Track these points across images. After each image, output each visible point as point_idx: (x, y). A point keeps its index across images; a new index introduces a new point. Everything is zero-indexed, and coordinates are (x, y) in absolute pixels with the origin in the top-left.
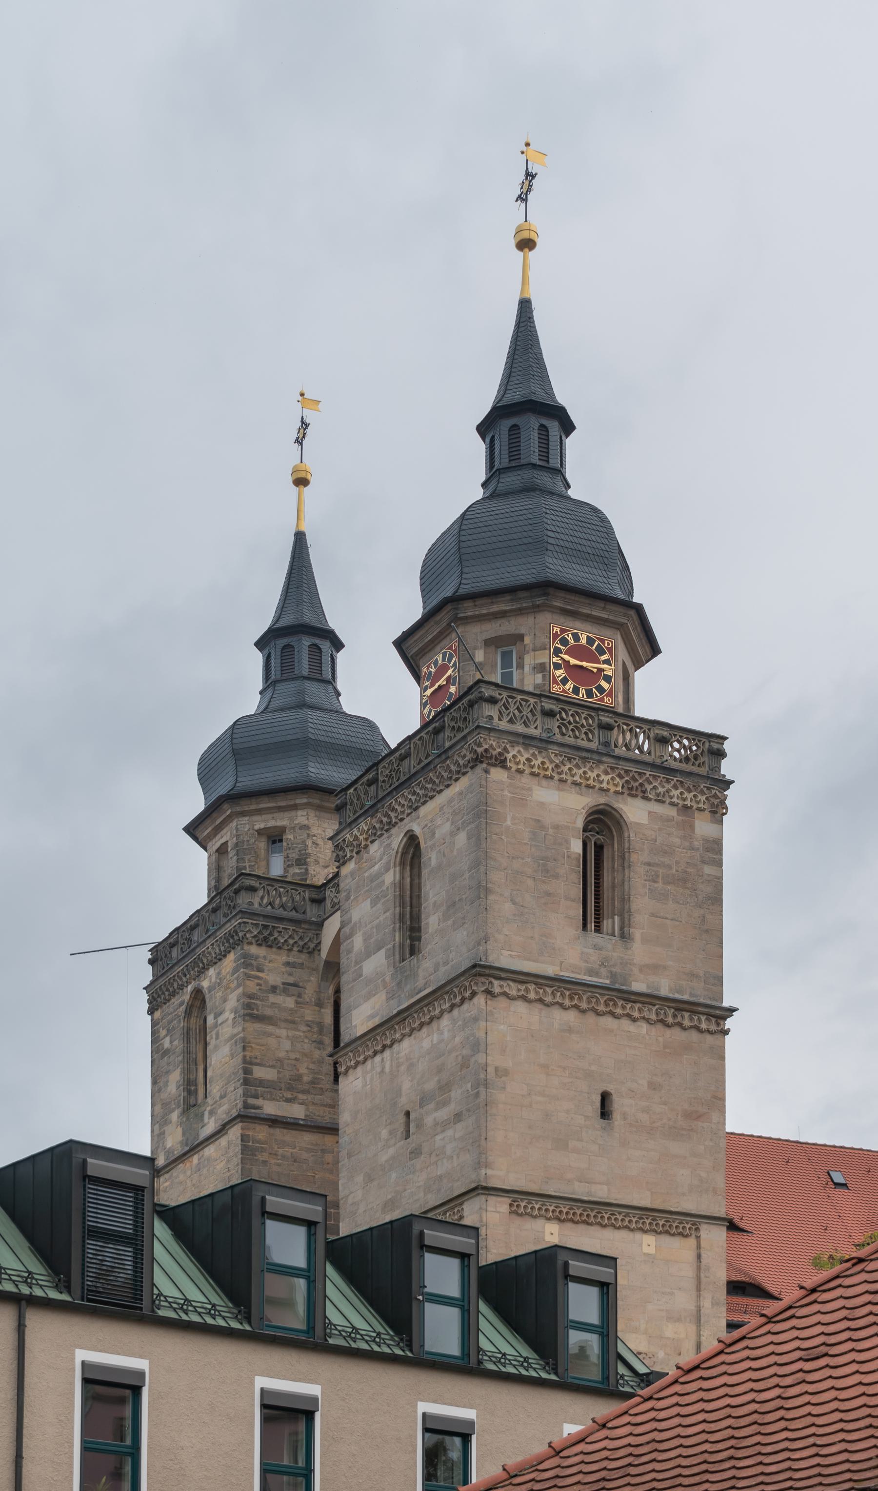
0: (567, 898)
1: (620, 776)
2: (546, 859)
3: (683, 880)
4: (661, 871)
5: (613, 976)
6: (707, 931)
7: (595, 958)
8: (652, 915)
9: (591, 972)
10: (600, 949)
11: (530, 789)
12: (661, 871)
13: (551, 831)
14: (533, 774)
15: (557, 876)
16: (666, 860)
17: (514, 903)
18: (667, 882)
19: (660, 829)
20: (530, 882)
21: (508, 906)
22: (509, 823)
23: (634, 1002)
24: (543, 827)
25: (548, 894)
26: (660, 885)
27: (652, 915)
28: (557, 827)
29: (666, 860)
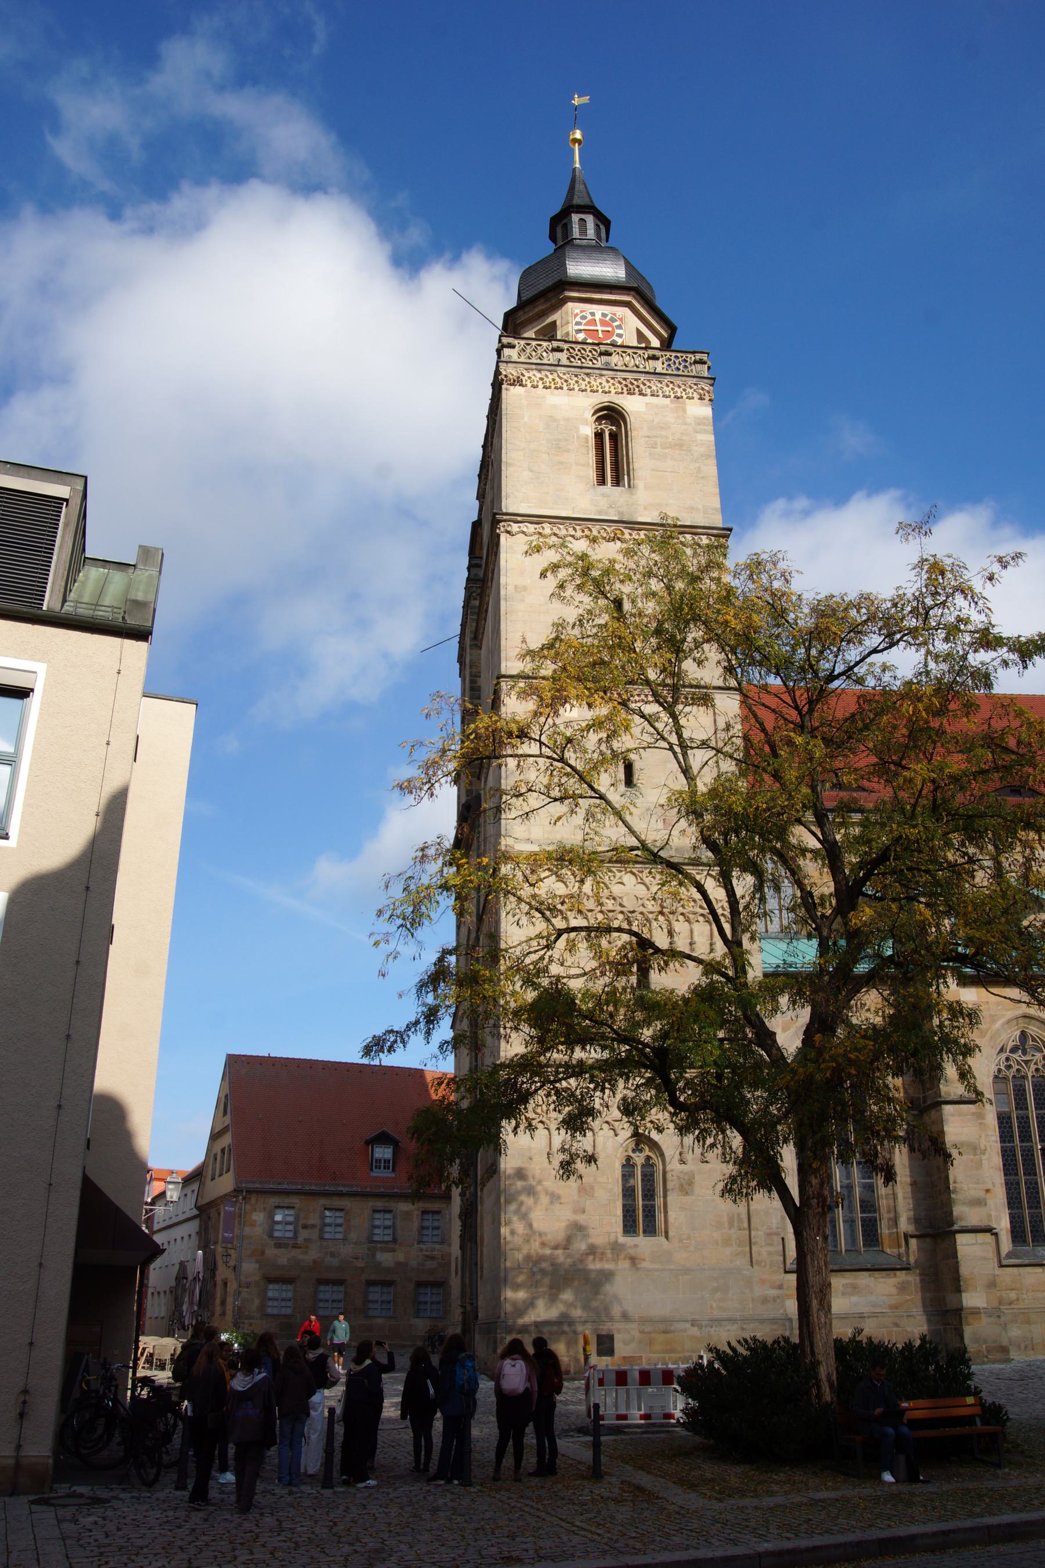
0: (577, 464)
1: (620, 383)
2: (559, 440)
3: (680, 445)
4: (659, 440)
5: (619, 513)
6: (703, 478)
7: (603, 503)
8: (654, 470)
9: (600, 512)
10: (608, 496)
11: (544, 397)
12: (659, 440)
13: (562, 422)
14: (545, 387)
15: (568, 451)
16: (663, 433)
17: (531, 471)
18: (664, 446)
19: (656, 414)
20: (545, 457)
21: (526, 475)
22: (526, 419)
23: (640, 530)
24: (555, 420)
25: (562, 463)
26: (659, 449)
27: (654, 470)
28: (567, 419)
29: (663, 433)
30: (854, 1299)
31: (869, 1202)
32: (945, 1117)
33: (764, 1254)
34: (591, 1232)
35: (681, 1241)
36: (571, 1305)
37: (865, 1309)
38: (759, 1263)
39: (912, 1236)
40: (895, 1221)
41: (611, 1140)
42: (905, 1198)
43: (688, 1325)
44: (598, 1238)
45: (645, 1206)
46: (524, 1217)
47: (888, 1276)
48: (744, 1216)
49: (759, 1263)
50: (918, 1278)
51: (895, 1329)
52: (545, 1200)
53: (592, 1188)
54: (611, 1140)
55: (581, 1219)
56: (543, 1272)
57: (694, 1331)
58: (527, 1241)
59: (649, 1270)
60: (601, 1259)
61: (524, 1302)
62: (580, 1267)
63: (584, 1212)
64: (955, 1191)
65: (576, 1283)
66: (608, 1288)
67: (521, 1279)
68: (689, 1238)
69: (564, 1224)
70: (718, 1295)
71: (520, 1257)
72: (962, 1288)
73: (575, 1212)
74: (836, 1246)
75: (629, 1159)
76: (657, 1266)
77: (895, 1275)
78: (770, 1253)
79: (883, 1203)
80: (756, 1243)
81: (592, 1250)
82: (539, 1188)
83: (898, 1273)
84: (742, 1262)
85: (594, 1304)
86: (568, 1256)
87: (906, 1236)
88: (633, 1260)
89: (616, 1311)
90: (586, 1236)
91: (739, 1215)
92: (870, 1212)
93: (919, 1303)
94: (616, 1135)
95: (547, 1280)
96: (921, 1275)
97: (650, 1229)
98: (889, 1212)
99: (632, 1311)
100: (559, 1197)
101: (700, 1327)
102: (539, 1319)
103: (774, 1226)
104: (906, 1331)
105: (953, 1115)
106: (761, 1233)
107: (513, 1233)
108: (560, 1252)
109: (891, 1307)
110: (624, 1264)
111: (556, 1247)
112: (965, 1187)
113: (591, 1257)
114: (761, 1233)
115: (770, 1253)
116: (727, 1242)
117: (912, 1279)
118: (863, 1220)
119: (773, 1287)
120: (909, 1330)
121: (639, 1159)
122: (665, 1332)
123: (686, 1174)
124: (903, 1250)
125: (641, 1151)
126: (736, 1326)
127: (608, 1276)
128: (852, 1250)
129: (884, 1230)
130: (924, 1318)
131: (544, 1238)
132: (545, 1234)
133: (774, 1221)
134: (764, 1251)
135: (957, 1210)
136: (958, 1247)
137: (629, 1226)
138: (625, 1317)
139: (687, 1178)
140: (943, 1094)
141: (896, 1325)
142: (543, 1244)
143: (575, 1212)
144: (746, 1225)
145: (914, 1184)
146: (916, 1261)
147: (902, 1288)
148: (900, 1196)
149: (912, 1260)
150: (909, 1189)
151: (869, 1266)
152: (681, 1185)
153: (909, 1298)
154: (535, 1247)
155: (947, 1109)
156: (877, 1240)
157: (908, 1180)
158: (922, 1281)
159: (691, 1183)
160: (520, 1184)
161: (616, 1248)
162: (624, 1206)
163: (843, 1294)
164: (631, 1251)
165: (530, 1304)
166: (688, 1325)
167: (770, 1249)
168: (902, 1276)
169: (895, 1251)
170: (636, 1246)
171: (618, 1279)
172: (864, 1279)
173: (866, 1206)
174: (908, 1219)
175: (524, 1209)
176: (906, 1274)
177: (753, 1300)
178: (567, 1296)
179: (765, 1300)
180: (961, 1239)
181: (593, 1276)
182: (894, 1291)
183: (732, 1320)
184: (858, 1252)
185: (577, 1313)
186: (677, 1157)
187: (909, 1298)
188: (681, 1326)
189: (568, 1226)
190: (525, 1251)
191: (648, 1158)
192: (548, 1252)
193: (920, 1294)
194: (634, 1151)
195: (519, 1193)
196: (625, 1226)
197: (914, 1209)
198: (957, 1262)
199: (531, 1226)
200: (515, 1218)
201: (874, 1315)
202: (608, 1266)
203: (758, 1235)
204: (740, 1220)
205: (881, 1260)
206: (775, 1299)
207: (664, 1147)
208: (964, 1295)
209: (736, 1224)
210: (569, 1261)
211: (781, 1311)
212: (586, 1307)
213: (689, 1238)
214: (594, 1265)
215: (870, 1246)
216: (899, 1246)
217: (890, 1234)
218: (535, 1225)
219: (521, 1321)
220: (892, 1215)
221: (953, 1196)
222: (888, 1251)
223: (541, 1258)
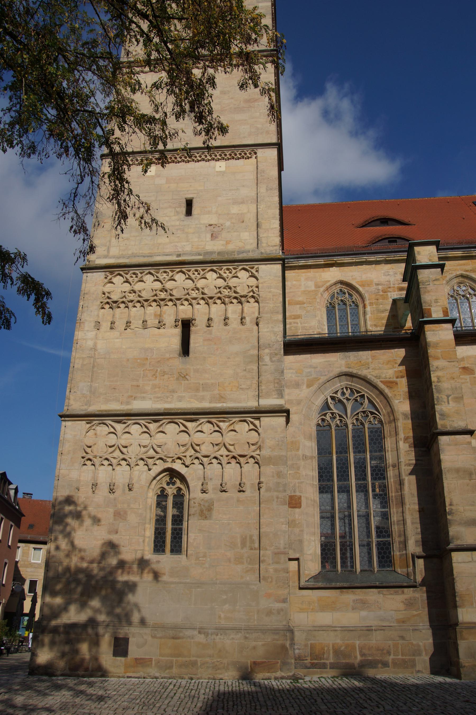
30: (364, 613)
31: (384, 528)
32: (441, 447)
33: (271, 570)
34: (122, 549)
35: (197, 558)
36: (97, 611)
37: (374, 623)
38: (265, 579)
39: (419, 557)
40: (404, 544)
41: (145, 473)
42: (413, 523)
43: (196, 632)
44: (128, 555)
45: (173, 530)
46: (68, 535)
47: (396, 593)
48: (256, 538)
49: (265, 579)
50: (425, 595)
51: (401, 642)
52: (88, 522)
53: (126, 513)
54: (145, 473)
55: (115, 538)
56: (78, 582)
57: (201, 638)
58: (68, 556)
59: (166, 583)
60: (129, 573)
61: (59, 606)
62: (111, 578)
63: (117, 532)
64: (451, 513)
65: (103, 592)
66: (131, 598)
67: (59, 587)
68: (205, 556)
69: (100, 543)
70: (227, 607)
71: (60, 569)
72: (458, 604)
73: (110, 532)
74: (352, 567)
75: (163, 490)
76: (176, 580)
77: (403, 592)
78: (276, 570)
79: (395, 529)
80: (264, 561)
81: (122, 564)
82: (84, 513)
83: (406, 590)
84: (251, 578)
85: (118, 610)
86: (102, 569)
87: (414, 557)
88: (156, 576)
89: (136, 617)
90: (117, 553)
91: (251, 537)
92: (384, 537)
93: (426, 618)
94: (150, 470)
95: (79, 589)
96: (427, 592)
97: (177, 548)
98: (400, 536)
99: (150, 620)
100: (99, 520)
101: (207, 634)
102: (69, 622)
103: (282, 546)
104: (412, 644)
105: (449, 445)
106: (269, 552)
107: (57, 548)
108: (95, 565)
109: (398, 621)
110: (148, 577)
111: (92, 562)
112: (461, 509)
113: (120, 571)
114: (269, 552)
115: (276, 570)
116: (239, 560)
117: (420, 595)
118: (378, 544)
119: (280, 602)
120: (414, 643)
121: (171, 491)
122: (173, 638)
123: (207, 501)
124: (411, 569)
125: (174, 484)
126: (239, 635)
127: (132, 587)
128: (368, 570)
129: (396, 553)
130: (430, 632)
131: (83, 554)
132: (85, 550)
133: (282, 542)
134: (271, 569)
135: (453, 530)
136: (454, 565)
137: (159, 546)
138: (143, 622)
139: (207, 504)
140: (439, 427)
141: (402, 638)
142: (82, 559)
143: (110, 532)
144: (257, 545)
145: (421, 511)
146: (423, 580)
147: (409, 604)
148: (409, 521)
149: (419, 578)
150: (417, 515)
151: (377, 584)
152: (202, 511)
153: (415, 613)
154: (74, 561)
155: (443, 440)
156: (390, 561)
157: (417, 507)
158: (428, 597)
159: (210, 509)
160: (68, 508)
161: (143, 563)
162: (156, 529)
163: (353, 609)
164: (154, 566)
165: (65, 608)
166: (196, 632)
167: (277, 566)
168: (409, 593)
169: (405, 570)
170: (158, 562)
171: (140, 590)
172: (372, 595)
173: (381, 532)
174: (416, 542)
175: (68, 529)
176: (414, 592)
177: (258, 611)
178: (95, 603)
179: (269, 613)
180: (456, 556)
181: (119, 586)
182: (402, 606)
183: (237, 630)
184: (372, 571)
185: (102, 618)
186: (200, 487)
187: (415, 613)
188: (189, 633)
189: (104, 544)
190: (65, 564)
191: (179, 489)
192: (85, 565)
193: (426, 609)
194: (168, 484)
195: (66, 516)
196: (155, 546)
197: (422, 533)
198: (453, 579)
199: (72, 544)
200: (60, 537)
201: (382, 629)
202: (133, 578)
203: (267, 554)
204: (252, 541)
205: (391, 579)
206: (279, 611)
207: (189, 480)
208: (460, 610)
209: (248, 544)
210: (102, 574)
211: (284, 623)
212: (109, 613)
213: (205, 556)
214: (122, 577)
215: (384, 566)
216: (408, 566)
217: (401, 555)
218: (76, 542)
219: (54, 623)
220: (402, 539)
221: (449, 517)
222: (399, 570)
223: (79, 570)
